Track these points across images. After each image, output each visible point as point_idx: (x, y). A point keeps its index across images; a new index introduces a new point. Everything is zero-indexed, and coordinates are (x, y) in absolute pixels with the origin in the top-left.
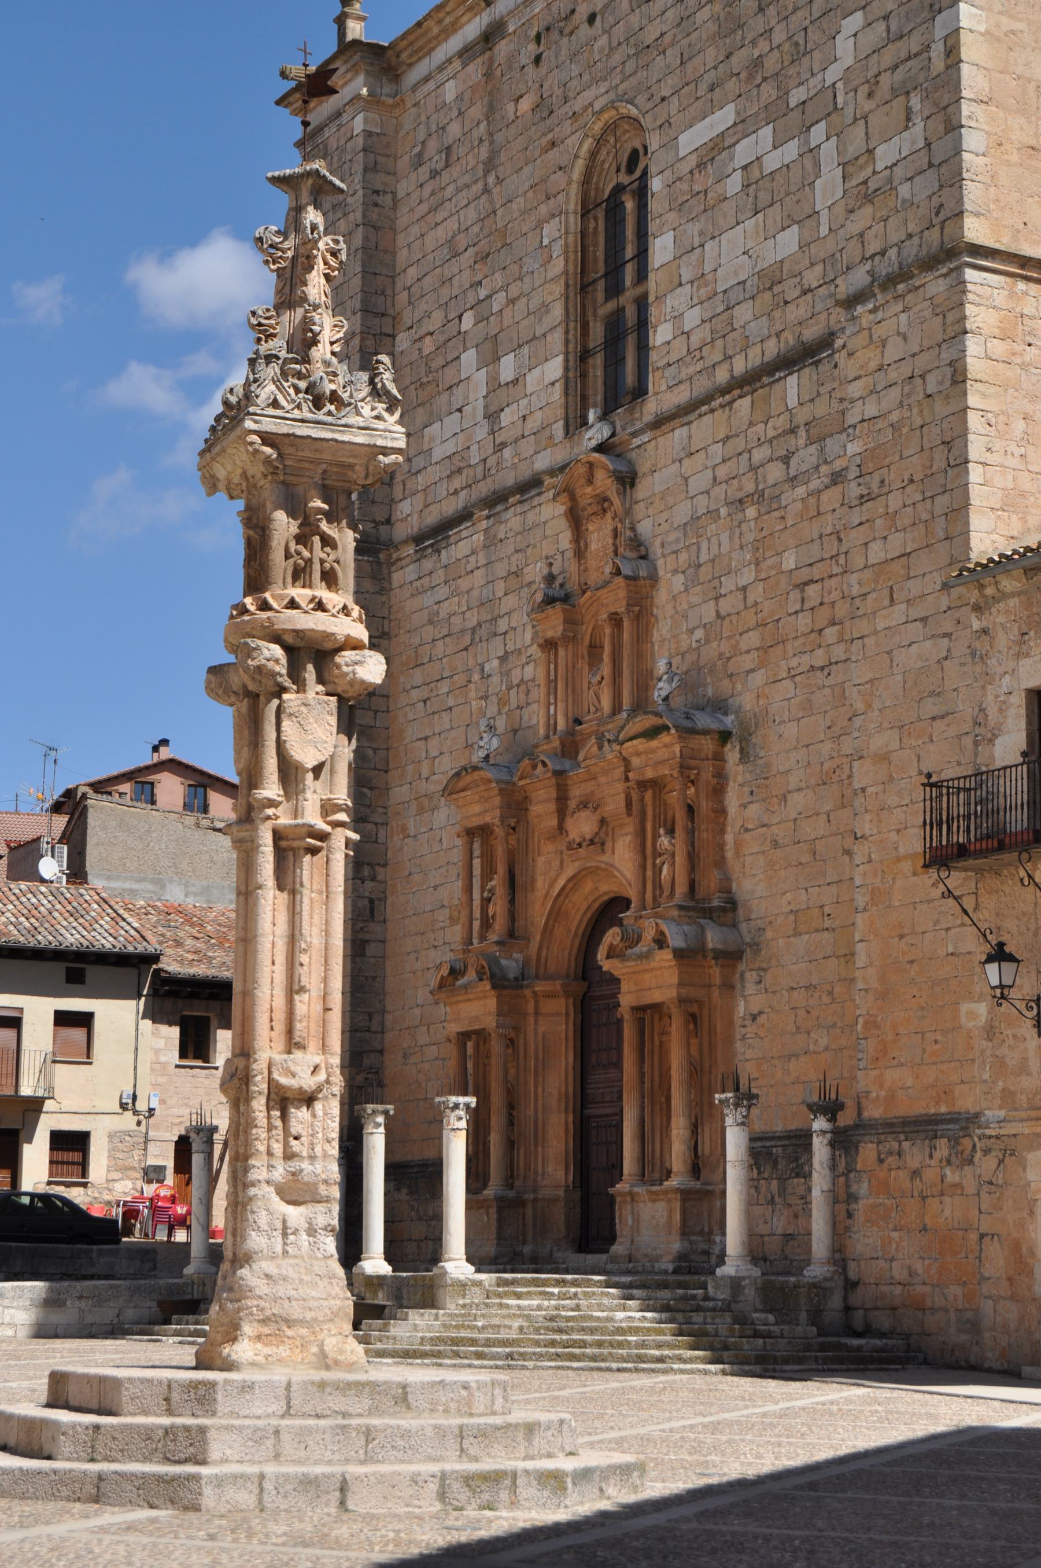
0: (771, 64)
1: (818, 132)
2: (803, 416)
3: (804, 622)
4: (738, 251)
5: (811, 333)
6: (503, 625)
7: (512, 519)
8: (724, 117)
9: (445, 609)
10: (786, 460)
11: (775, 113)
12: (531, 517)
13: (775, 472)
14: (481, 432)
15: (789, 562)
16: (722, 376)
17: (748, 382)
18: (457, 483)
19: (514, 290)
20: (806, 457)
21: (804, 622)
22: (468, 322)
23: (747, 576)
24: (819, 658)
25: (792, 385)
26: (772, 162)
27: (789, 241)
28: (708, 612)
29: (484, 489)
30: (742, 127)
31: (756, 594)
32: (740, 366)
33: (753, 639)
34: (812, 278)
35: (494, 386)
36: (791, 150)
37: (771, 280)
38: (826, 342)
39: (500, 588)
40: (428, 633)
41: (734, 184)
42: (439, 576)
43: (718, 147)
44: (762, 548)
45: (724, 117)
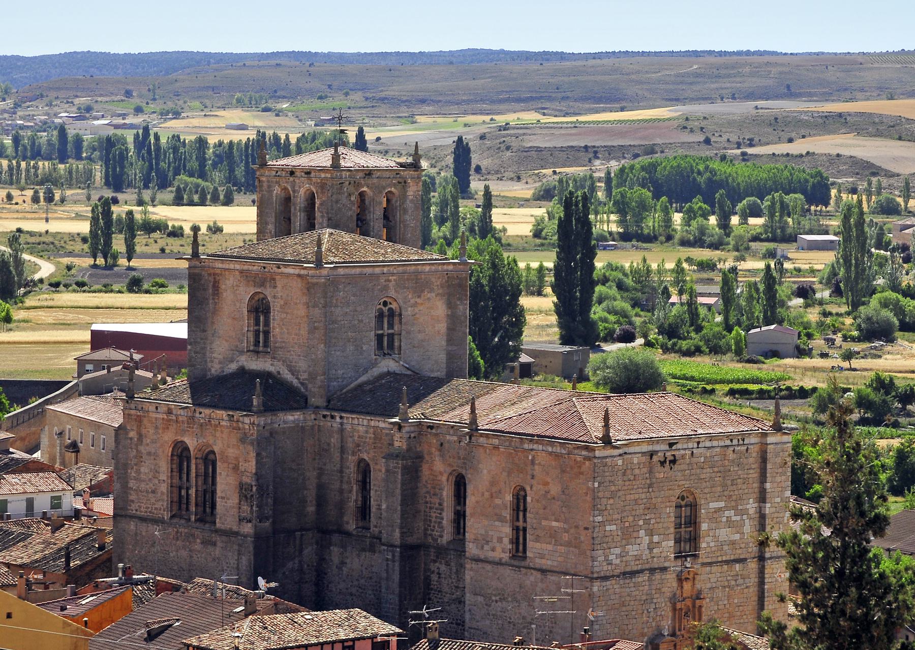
0: (734, 498)
1: (745, 517)
2: (740, 573)
3: (739, 614)
4: (724, 534)
5: (742, 557)
6: (655, 601)
7: (657, 576)
8: (722, 504)
9: (634, 593)
10: (736, 581)
11: (735, 508)
12: (663, 577)
13: (733, 583)
14: (647, 552)
15: (736, 601)
16: (720, 559)
17: (727, 562)
18: (638, 562)
19: (658, 520)
20: (740, 581)
21: (739, 614)
22: (641, 522)
23: (726, 602)
24: (742, 621)
25: (737, 565)
26: (734, 518)
27: (737, 537)
28: (716, 608)
29: (647, 566)
30: (727, 508)
31: (727, 606)
32: (724, 558)
33: (727, 615)
34: (743, 546)
35: (651, 542)
36: (738, 518)
37: (733, 543)
38: (745, 559)
39: (654, 592)
40: (628, 598)
41: (724, 519)
42: (632, 585)
43: (720, 509)
44: (729, 597)
45: (722, 504)
